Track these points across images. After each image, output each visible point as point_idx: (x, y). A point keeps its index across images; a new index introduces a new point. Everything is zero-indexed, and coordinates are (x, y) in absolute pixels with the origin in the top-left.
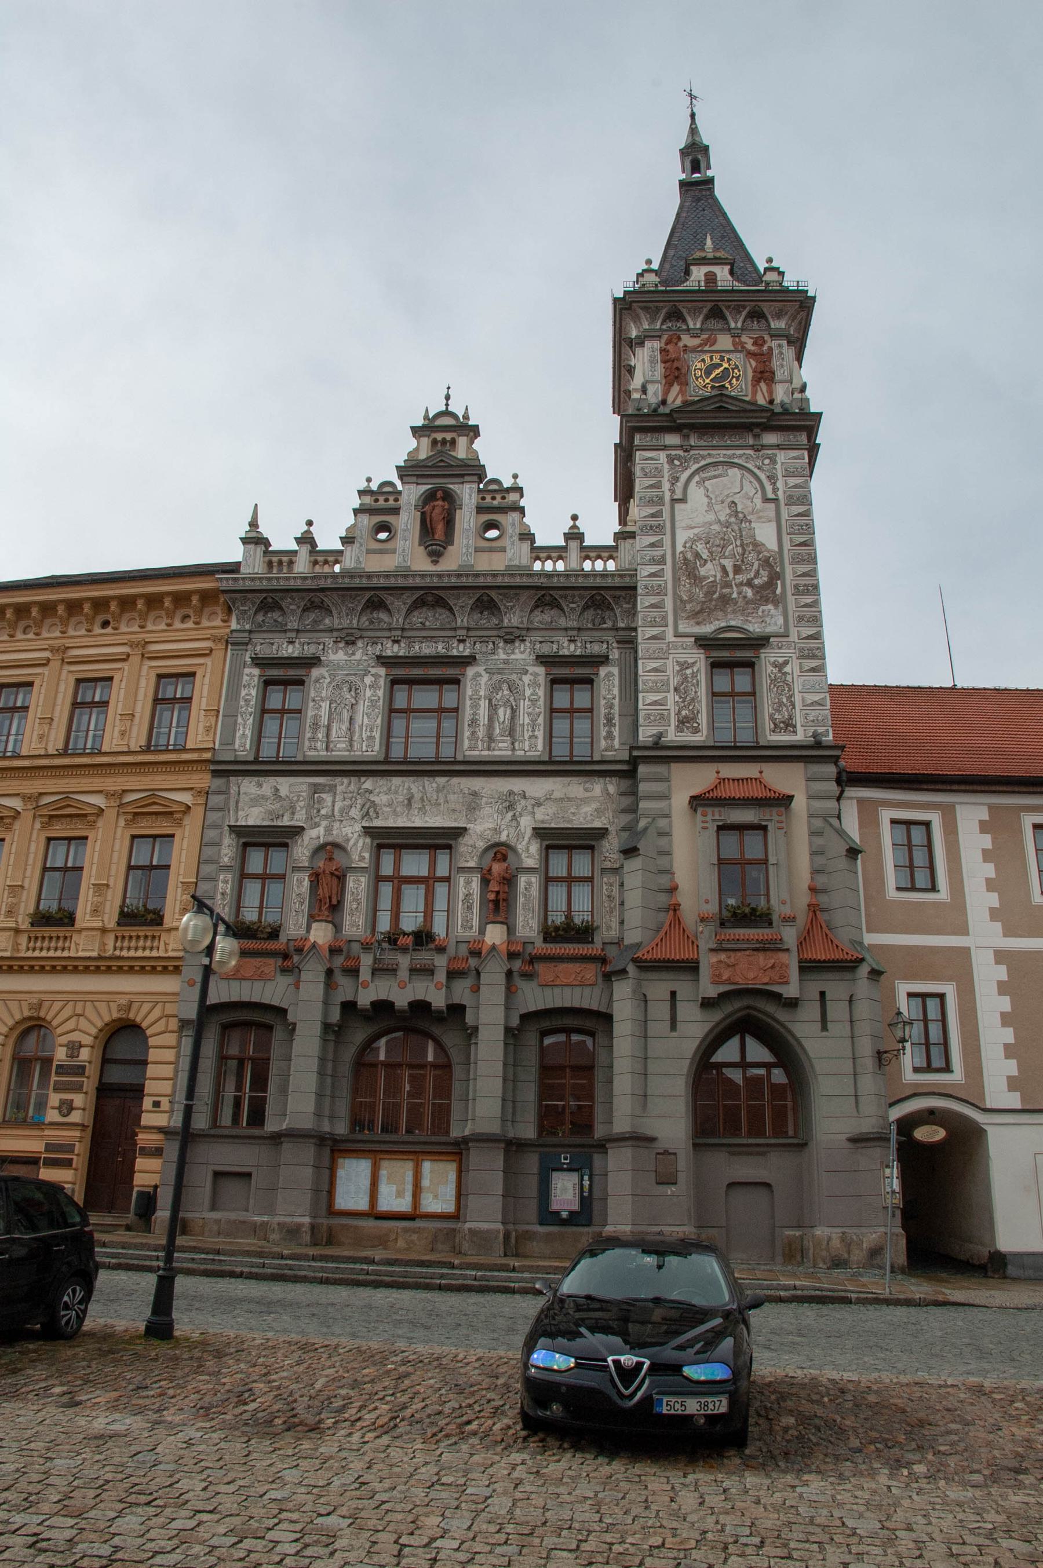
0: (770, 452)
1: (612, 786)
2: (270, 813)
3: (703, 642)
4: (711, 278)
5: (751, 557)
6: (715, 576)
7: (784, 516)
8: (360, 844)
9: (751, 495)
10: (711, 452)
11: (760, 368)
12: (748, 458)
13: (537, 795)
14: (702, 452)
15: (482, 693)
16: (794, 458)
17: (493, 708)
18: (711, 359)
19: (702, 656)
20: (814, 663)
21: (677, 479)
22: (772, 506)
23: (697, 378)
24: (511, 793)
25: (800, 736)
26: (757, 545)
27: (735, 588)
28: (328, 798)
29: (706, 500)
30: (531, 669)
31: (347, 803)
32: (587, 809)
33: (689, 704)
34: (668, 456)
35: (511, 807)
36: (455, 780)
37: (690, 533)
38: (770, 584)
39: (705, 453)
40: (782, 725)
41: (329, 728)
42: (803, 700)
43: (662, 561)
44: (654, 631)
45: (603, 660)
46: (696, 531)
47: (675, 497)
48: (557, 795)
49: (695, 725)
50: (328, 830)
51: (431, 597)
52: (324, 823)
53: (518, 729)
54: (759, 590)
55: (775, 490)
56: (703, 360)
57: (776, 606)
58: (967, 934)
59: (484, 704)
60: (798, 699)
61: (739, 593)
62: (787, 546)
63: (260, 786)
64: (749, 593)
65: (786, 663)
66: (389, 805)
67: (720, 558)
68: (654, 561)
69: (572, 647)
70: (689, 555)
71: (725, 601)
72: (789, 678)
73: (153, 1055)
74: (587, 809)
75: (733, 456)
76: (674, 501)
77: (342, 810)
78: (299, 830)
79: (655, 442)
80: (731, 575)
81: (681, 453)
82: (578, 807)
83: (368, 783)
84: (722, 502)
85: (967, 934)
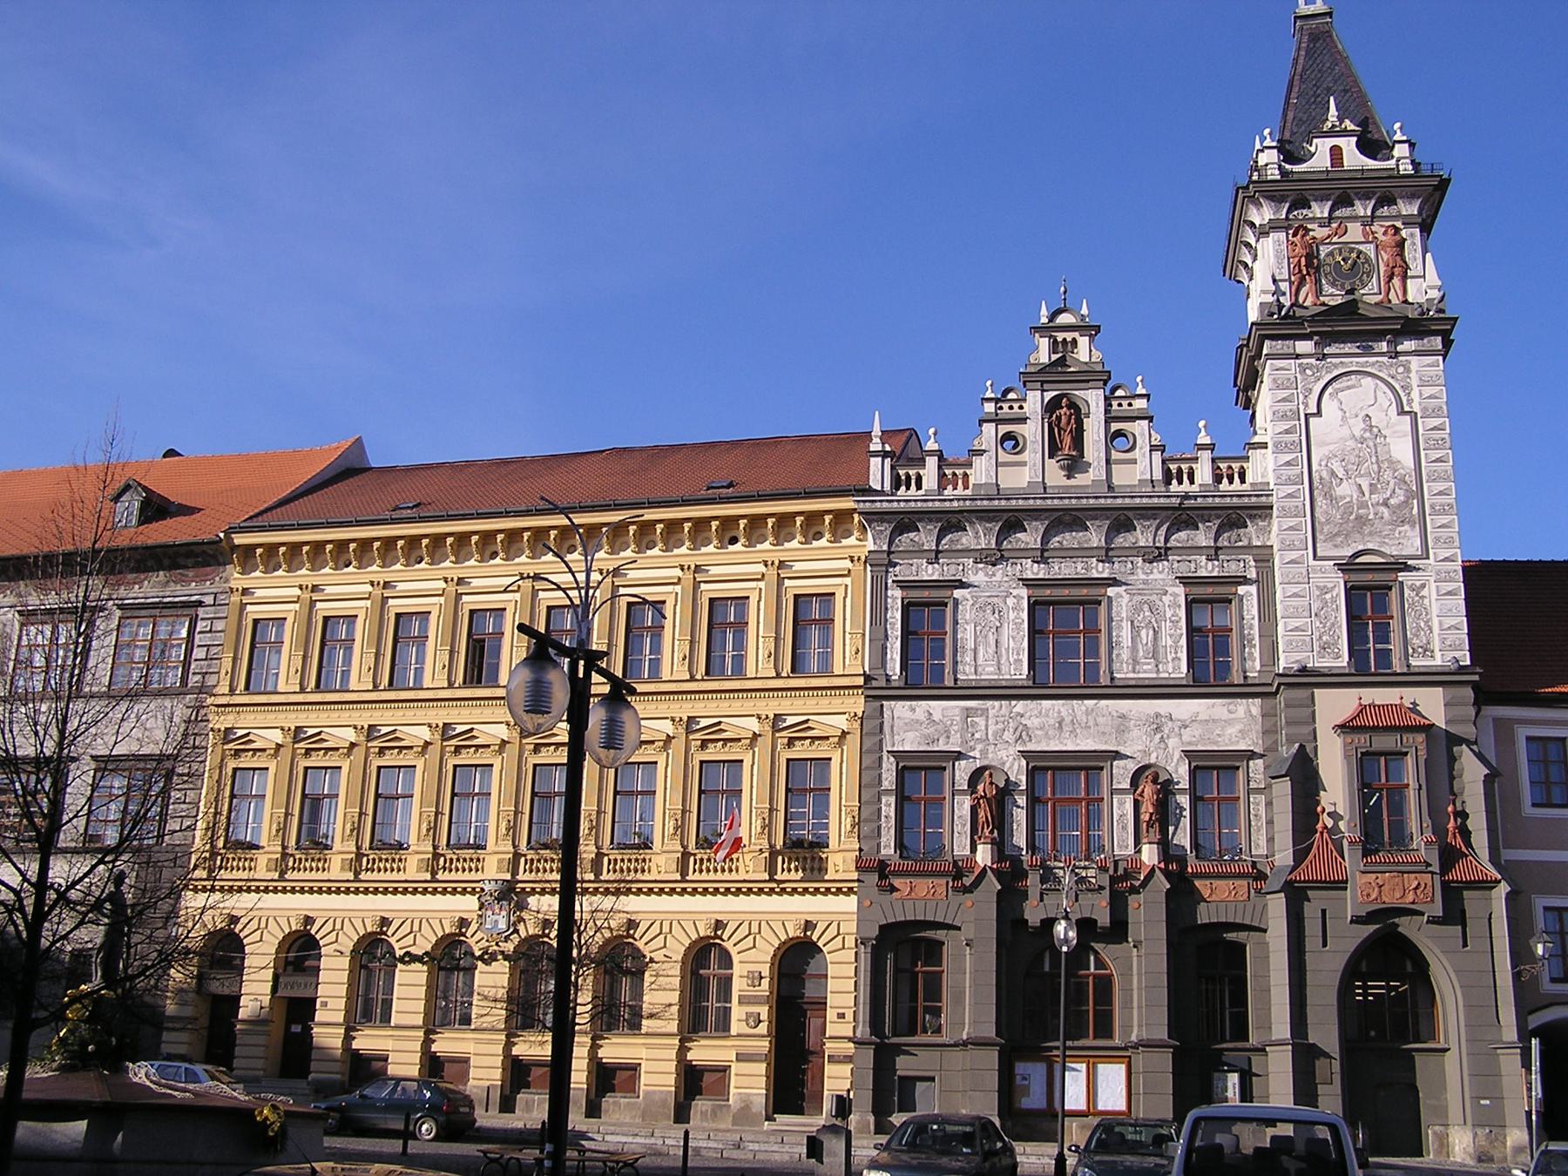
1: (1255, 705)
2: (926, 737)
4: (1336, 153)
5: (1388, 475)
24: (1158, 715)
26: (1391, 462)
28: (980, 721)
30: (1170, 590)
31: (1001, 726)
32: (1232, 731)
35: (1158, 729)
36: (1103, 702)
37: (1325, 451)
41: (975, 651)
42: (1441, 623)
44: (1294, 555)
46: (1331, 447)
50: (984, 753)
51: (1067, 519)
52: (979, 747)
53: (1161, 650)
54: (1395, 510)
55: (1410, 402)
57: (1413, 526)
59: (1126, 626)
63: (913, 710)
64: (1385, 512)
65: (1423, 586)
68: (1289, 481)
70: (1325, 474)
71: (1362, 521)
73: (831, 971)
74: (1232, 731)
77: (995, 734)
78: (959, 756)
79: (1286, 350)
81: (1313, 361)
83: (1020, 706)
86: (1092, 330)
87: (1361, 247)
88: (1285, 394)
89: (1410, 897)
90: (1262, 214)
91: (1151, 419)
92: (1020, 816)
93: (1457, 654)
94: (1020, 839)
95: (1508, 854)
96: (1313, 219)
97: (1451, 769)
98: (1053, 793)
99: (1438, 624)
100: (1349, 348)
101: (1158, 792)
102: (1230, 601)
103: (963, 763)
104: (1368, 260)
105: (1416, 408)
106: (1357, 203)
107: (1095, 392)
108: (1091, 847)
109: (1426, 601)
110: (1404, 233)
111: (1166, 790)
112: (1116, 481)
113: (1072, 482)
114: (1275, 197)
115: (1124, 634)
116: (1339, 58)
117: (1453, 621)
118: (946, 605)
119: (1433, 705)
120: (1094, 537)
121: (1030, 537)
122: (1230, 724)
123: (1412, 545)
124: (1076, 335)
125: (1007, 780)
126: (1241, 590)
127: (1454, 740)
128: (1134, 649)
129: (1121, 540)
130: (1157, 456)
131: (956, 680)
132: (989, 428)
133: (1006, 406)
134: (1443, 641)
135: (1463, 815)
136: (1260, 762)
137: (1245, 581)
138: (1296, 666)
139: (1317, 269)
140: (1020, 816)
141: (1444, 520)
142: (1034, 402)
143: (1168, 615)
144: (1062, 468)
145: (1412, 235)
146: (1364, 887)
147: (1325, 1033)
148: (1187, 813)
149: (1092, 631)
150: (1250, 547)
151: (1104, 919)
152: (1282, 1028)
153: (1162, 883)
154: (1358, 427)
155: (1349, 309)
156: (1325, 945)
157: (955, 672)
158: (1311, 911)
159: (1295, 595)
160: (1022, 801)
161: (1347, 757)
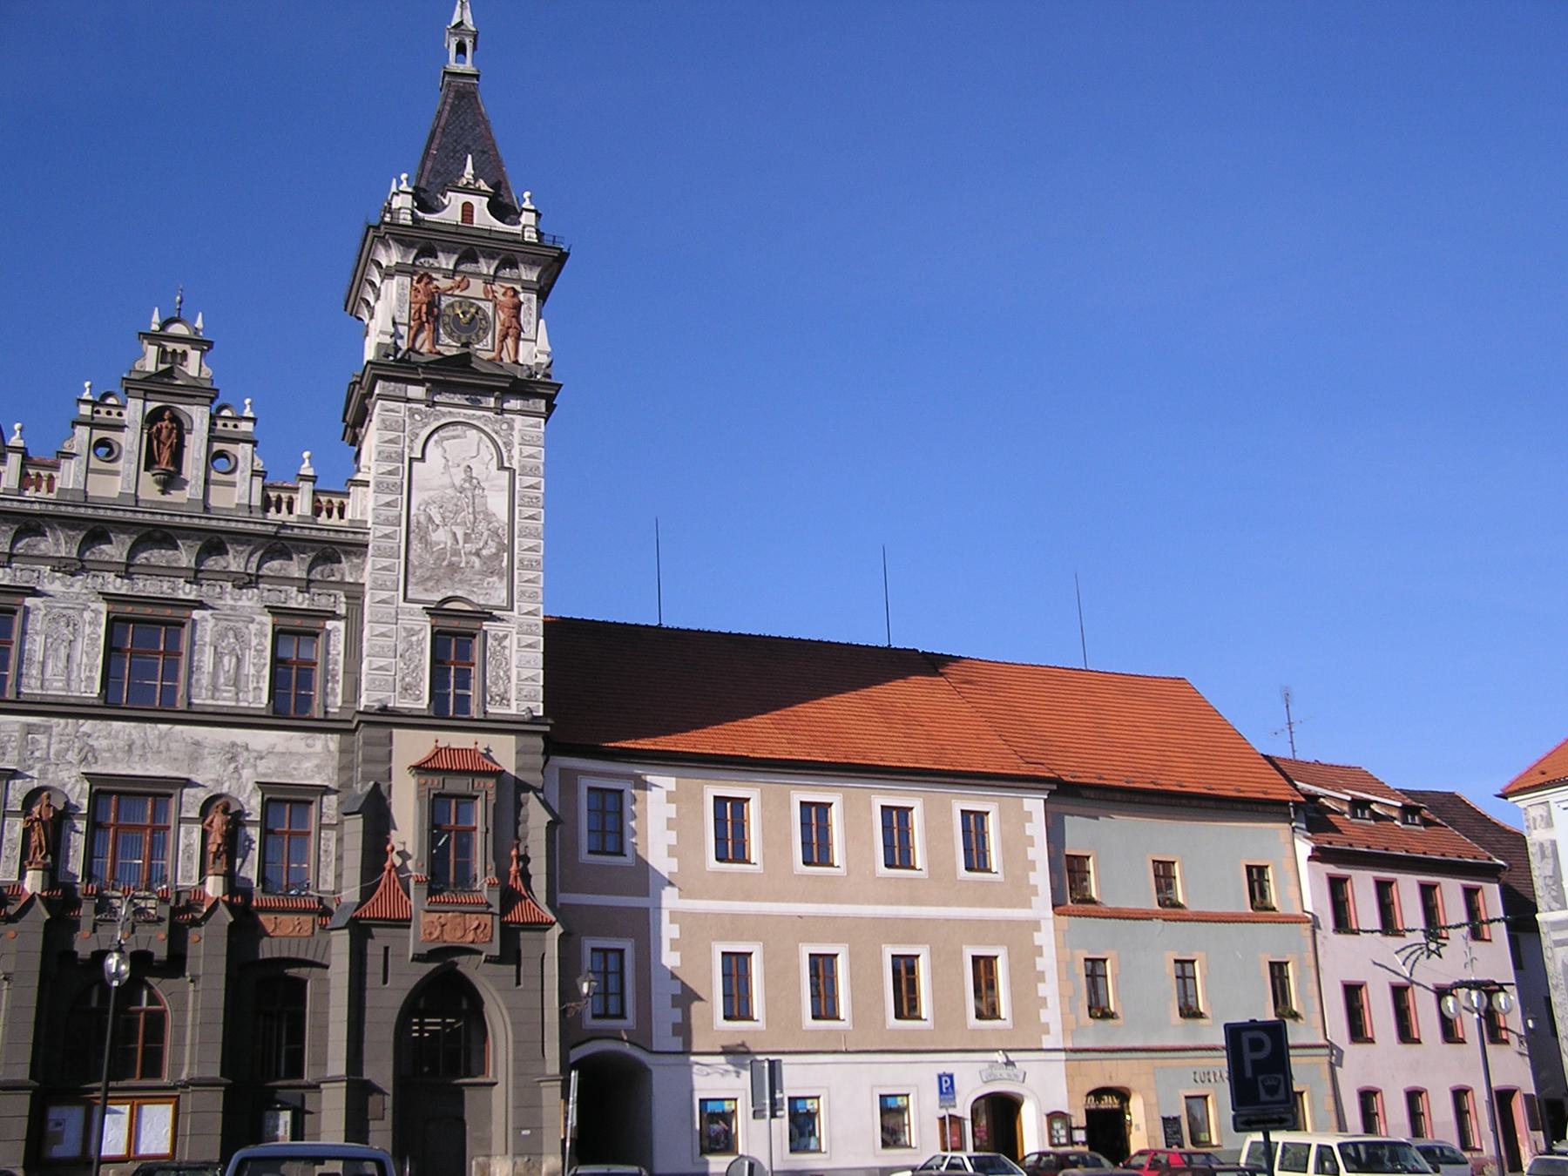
1: (333, 741)
4: (467, 209)
5: (482, 526)
8: (78, 789)
13: (259, 748)
15: (207, 639)
17: (218, 656)
21: (417, 435)
22: (506, 474)
24: (234, 745)
25: (513, 710)
26: (489, 516)
28: (42, 739)
30: (258, 618)
31: (64, 745)
32: (308, 765)
35: (233, 759)
36: (178, 728)
37: (425, 496)
41: (43, 664)
44: (384, 595)
48: (279, 749)
50: (43, 773)
52: (38, 766)
53: (243, 679)
55: (510, 458)
57: (501, 578)
58: (648, 895)
65: (505, 637)
66: (109, 750)
68: (387, 522)
70: (422, 519)
71: (453, 568)
74: (308, 765)
75: (470, 417)
77: (57, 754)
78: (14, 774)
79: (397, 393)
81: (422, 407)
82: (299, 762)
83: (87, 726)
85: (648, 895)
86: (204, 345)
87: (481, 304)
88: (392, 435)
89: (470, 937)
90: (389, 256)
91: (255, 443)
92: (78, 842)
93: (532, 705)
94: (76, 866)
95: (563, 898)
96: (438, 269)
97: (517, 813)
98: (117, 817)
99: (516, 674)
100: (458, 399)
101: (228, 823)
102: (317, 635)
103: (18, 782)
104: (485, 317)
105: (515, 465)
106: (482, 260)
107: (201, 409)
108: (153, 876)
110: (522, 297)
111: (236, 821)
112: (212, 502)
113: (166, 498)
114: (405, 242)
115: (206, 659)
116: (481, 120)
117: (530, 673)
118: (14, 612)
119: (505, 752)
120: (185, 557)
121: (115, 550)
122: (306, 758)
123: (499, 596)
124: (187, 347)
125: (67, 803)
126: (330, 625)
127: (522, 787)
128: (215, 675)
129: (212, 563)
130: (258, 482)
131: (18, 693)
132: (82, 433)
133: (103, 410)
134: (519, 691)
135: (524, 859)
136: (334, 798)
137: (334, 616)
138: (377, 705)
139: (437, 318)
140: (78, 842)
141: (531, 575)
142: (134, 411)
143: (254, 642)
144: (157, 482)
145: (529, 300)
146: (428, 925)
147: (380, 1070)
148: (256, 846)
149: (172, 653)
150: (341, 583)
151: (161, 952)
152: (337, 1065)
153: (225, 917)
154: (459, 477)
155: (463, 362)
156: (385, 982)
157: (18, 685)
158: (374, 948)
159: (382, 635)
160: (81, 825)
161: (419, 798)
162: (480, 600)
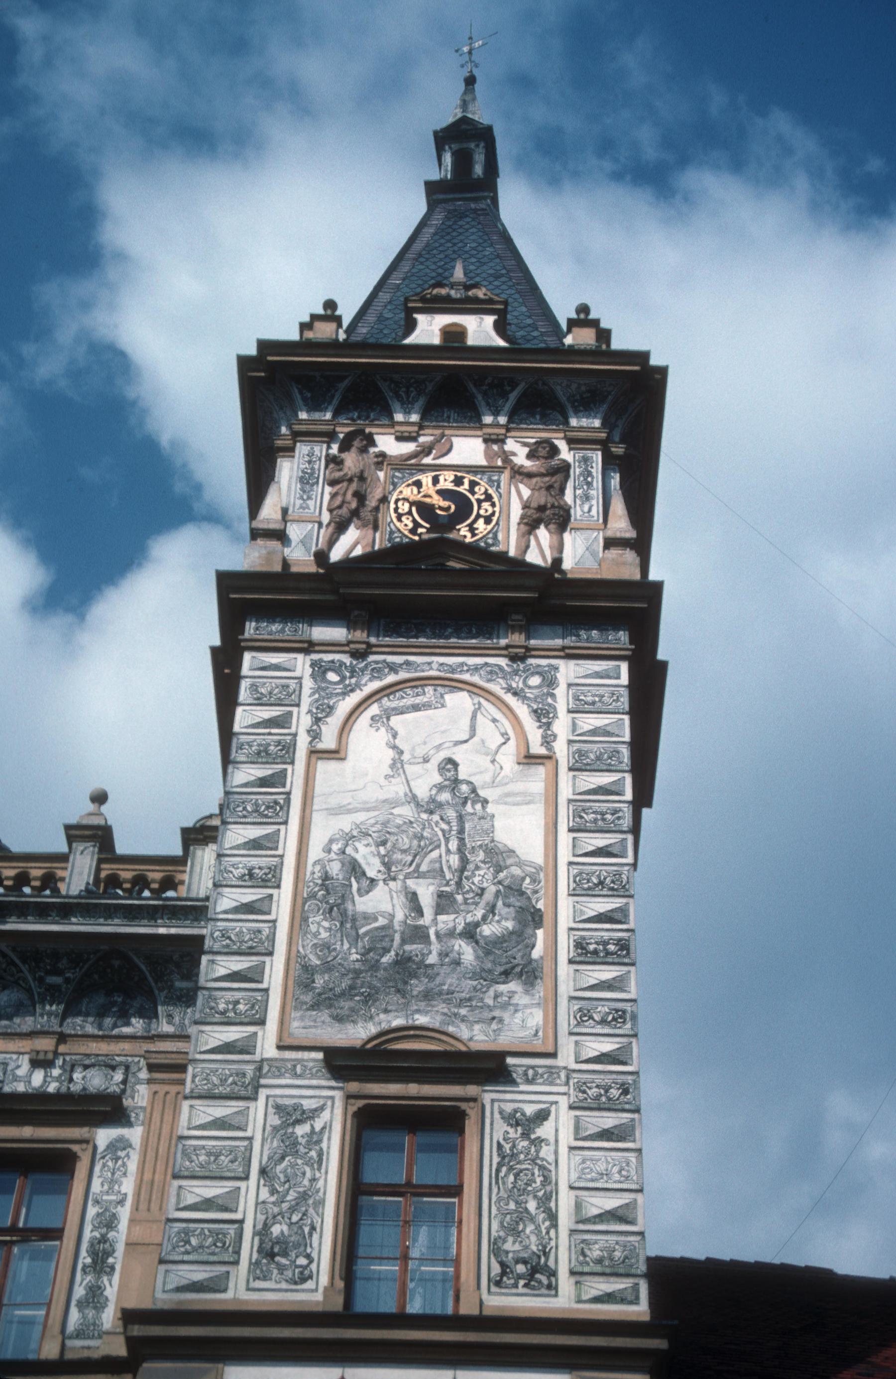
0: (544, 662)
3: (342, 1063)
5: (482, 877)
6: (392, 916)
7: (566, 791)
9: (494, 747)
10: (412, 658)
11: (542, 498)
12: (493, 673)
14: (390, 659)
16: (597, 675)
18: (436, 481)
19: (338, 1095)
20: (609, 1120)
21: (330, 710)
22: (541, 771)
23: (399, 517)
27: (435, 947)
29: (391, 753)
33: (292, 1210)
34: (313, 664)
37: (345, 823)
38: (521, 937)
39: (398, 659)
40: (521, 1268)
42: (578, 1206)
43: (271, 878)
45: (111, 1110)
46: (360, 817)
47: (320, 746)
49: (302, 1261)
55: (548, 740)
56: (418, 484)
60: (565, 1203)
61: (443, 955)
62: (564, 854)
64: (468, 953)
65: (542, 1116)
67: (407, 876)
68: (250, 878)
69: (38, 1078)
70: (335, 869)
71: (406, 968)
72: (546, 1152)
76: (315, 754)
80: (428, 913)
81: (347, 659)
84: (426, 760)
109: (546, 1152)
145: (586, 460)
154: (425, 782)
162: (476, 1036)
